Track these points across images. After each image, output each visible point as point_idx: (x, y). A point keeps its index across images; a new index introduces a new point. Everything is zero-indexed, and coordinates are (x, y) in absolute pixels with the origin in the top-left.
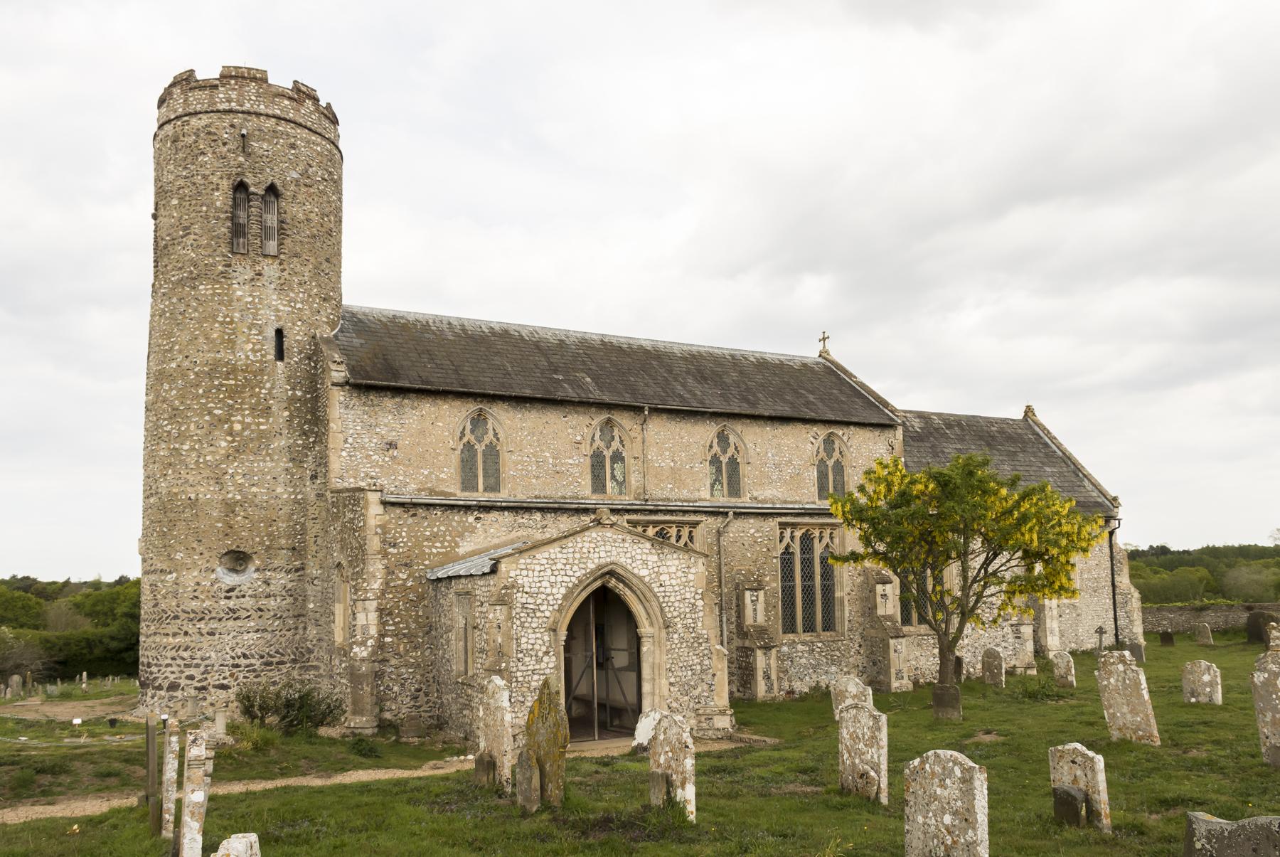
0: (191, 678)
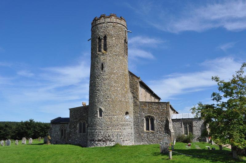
0: (122, 138)
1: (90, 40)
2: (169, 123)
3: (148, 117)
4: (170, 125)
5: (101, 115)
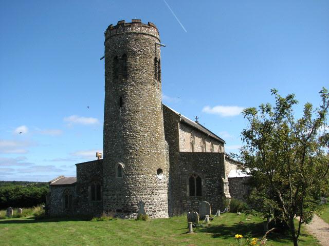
1: (104, 59)
2: (224, 184)
3: (194, 176)
4: (225, 188)
5: (120, 175)
